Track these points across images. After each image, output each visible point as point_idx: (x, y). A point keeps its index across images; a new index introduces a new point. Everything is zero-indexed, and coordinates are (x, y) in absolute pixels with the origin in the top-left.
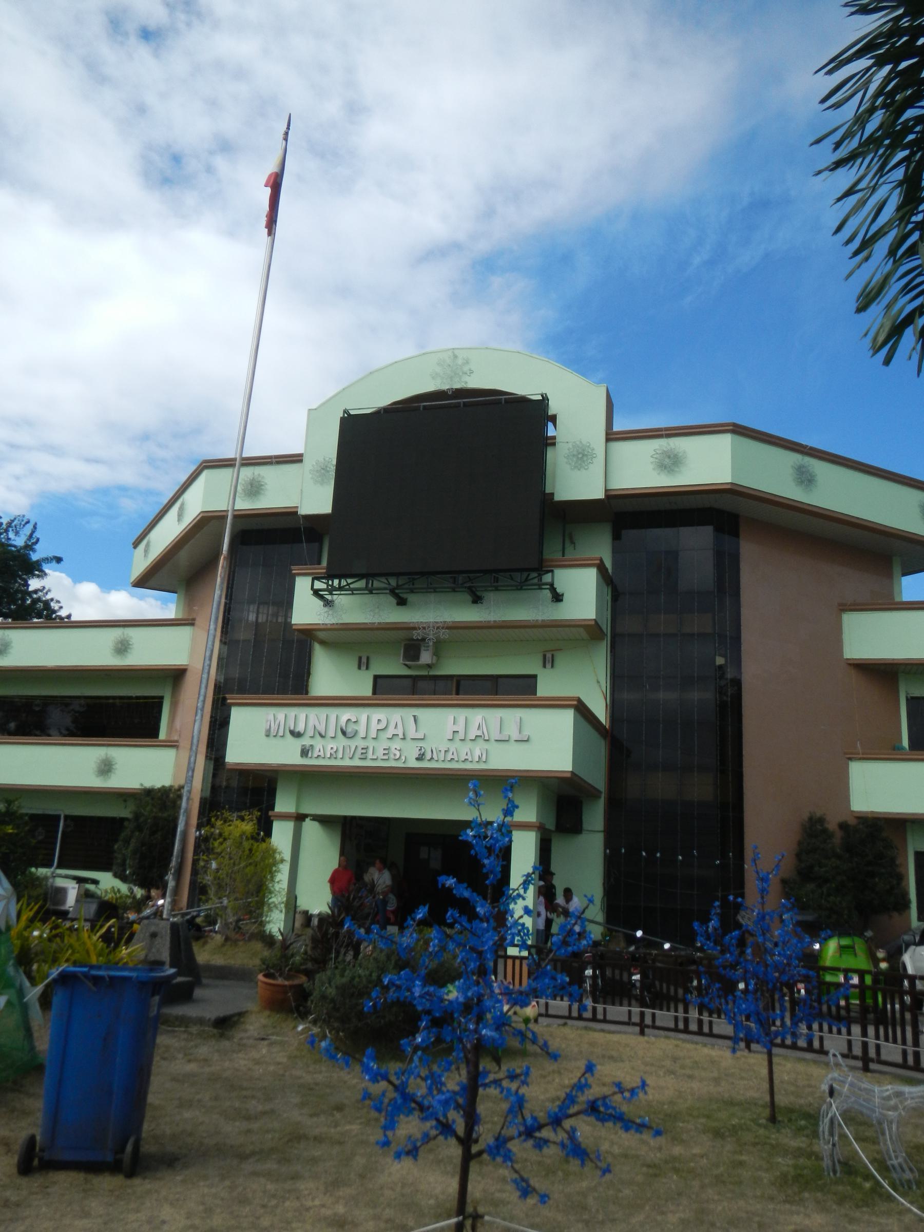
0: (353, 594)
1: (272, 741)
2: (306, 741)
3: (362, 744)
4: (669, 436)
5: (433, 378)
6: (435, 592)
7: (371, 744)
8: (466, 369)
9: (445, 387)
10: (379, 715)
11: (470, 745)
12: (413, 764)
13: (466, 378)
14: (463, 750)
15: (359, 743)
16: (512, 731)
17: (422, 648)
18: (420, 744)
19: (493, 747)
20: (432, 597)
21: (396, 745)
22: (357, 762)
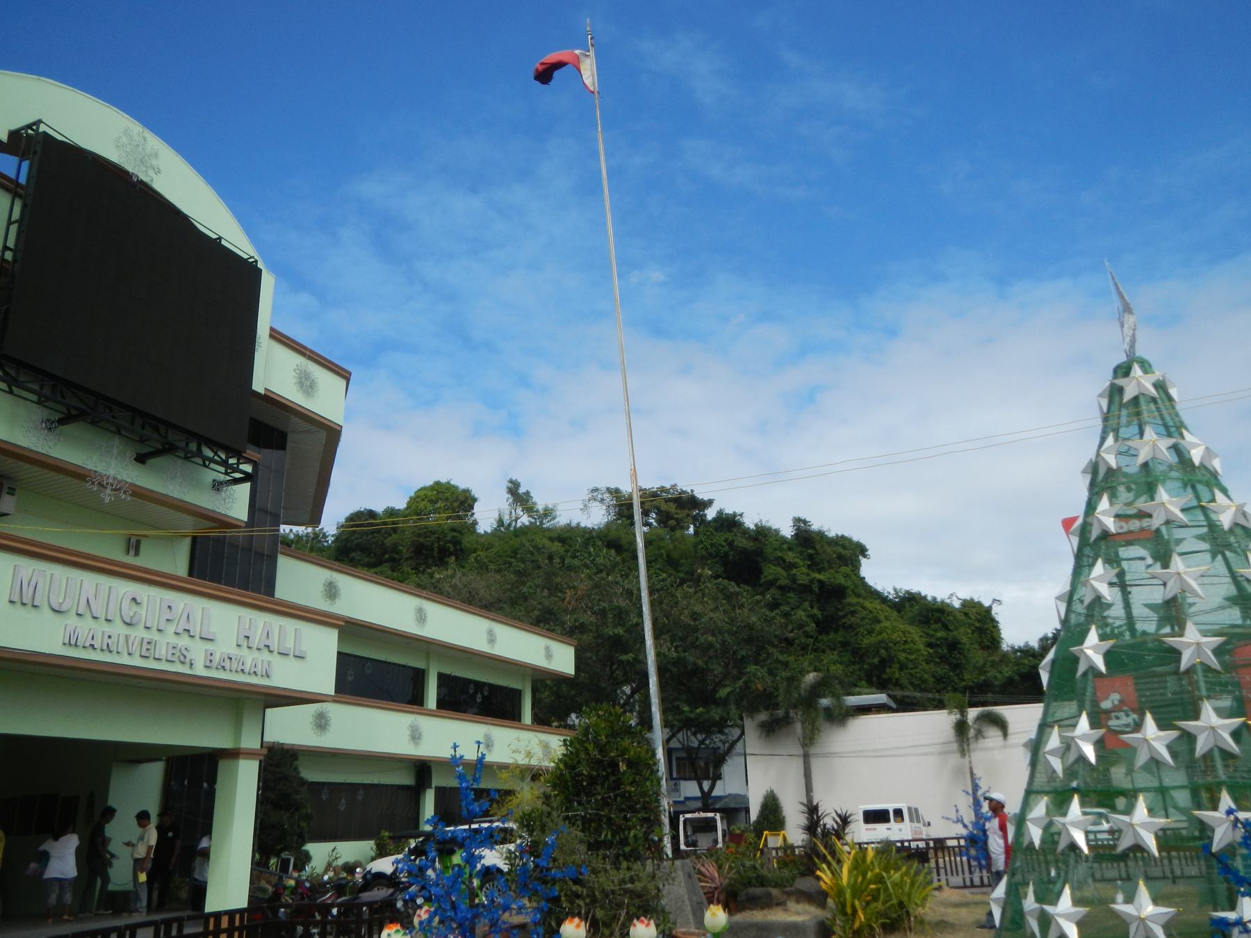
0: (11, 392)
1: (20, 611)
2: (72, 621)
3: (147, 635)
4: (310, 358)
5: (117, 147)
6: (119, 433)
7: (154, 636)
8: (154, 162)
9: (130, 170)
10: (181, 601)
11: (256, 654)
12: (200, 671)
13: (151, 173)
14: (249, 658)
15: (138, 633)
16: (290, 644)
17: (5, 490)
18: (209, 646)
19: (276, 659)
20: (117, 441)
21: (184, 641)
22: (137, 662)
